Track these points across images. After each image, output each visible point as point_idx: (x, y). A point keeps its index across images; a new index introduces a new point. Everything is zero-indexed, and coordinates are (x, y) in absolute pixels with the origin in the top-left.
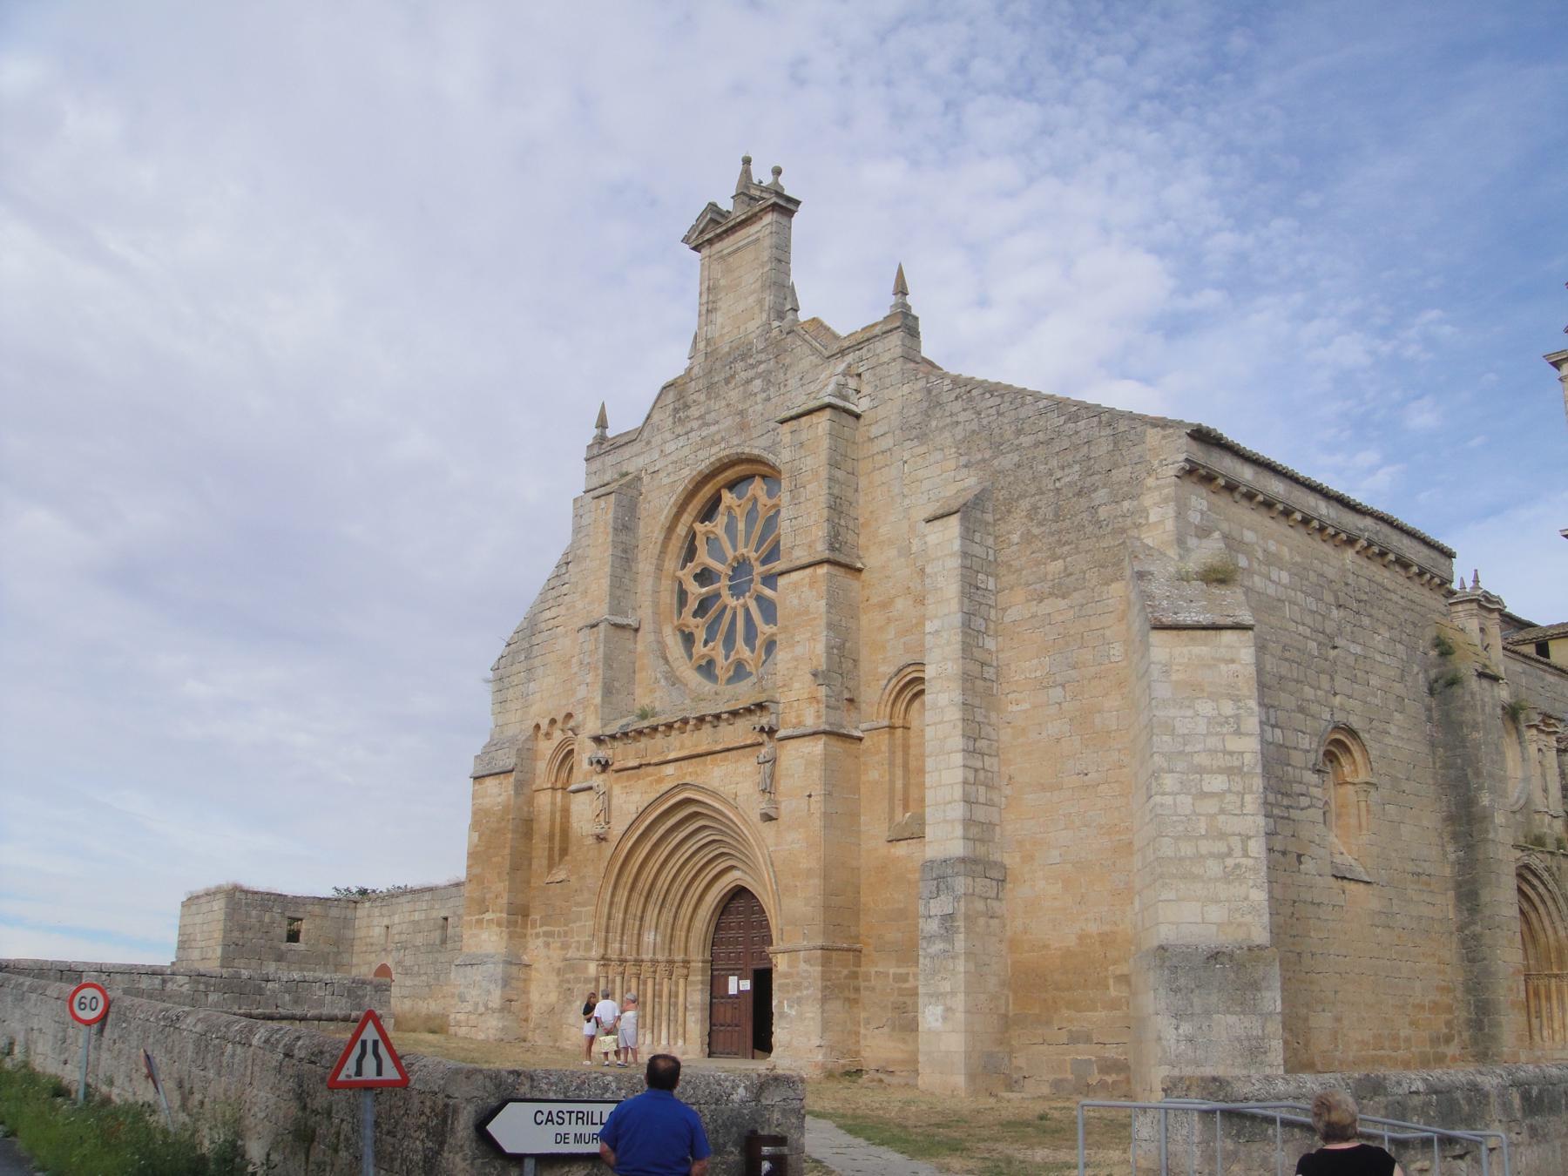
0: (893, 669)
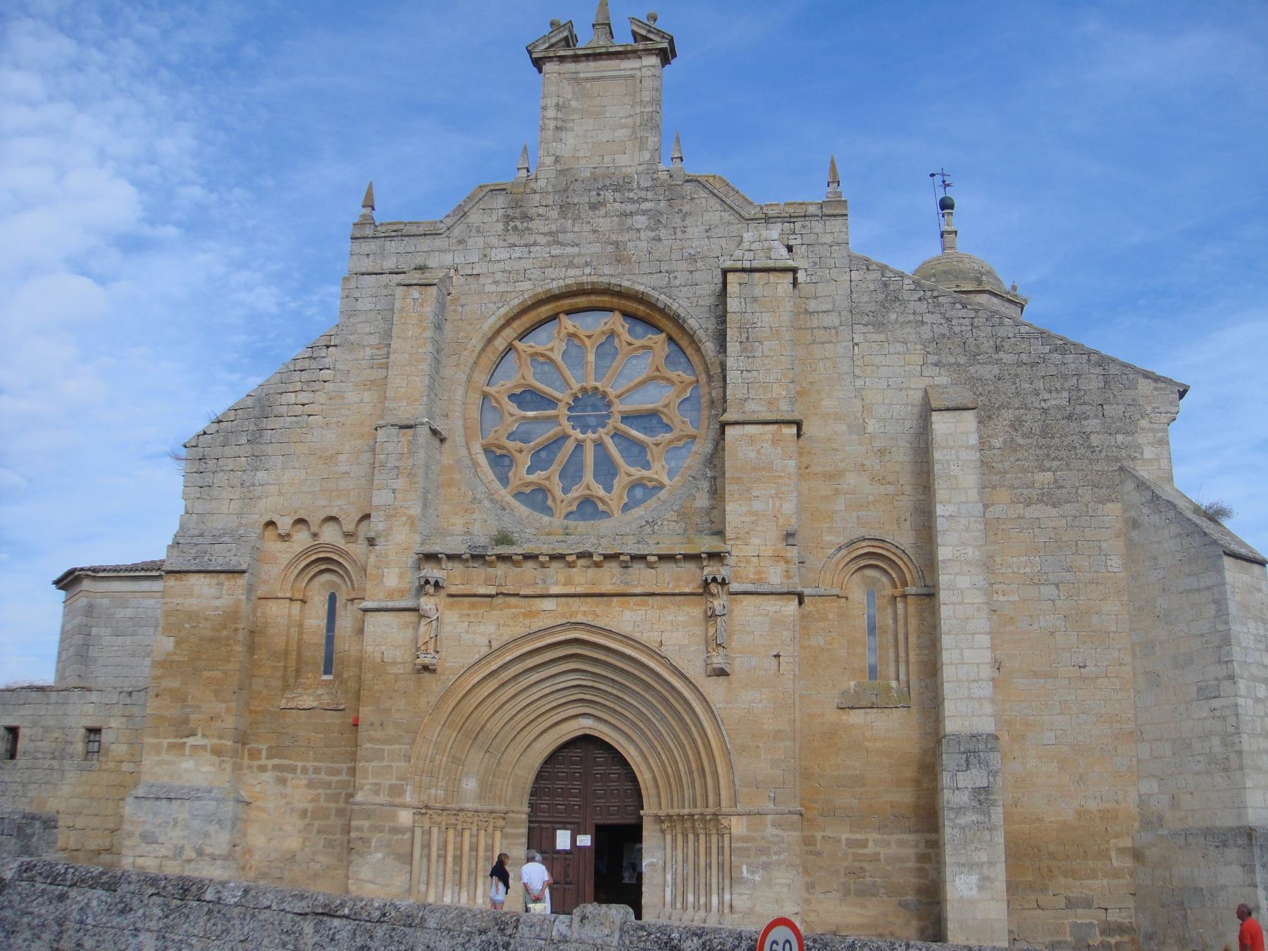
0: (842, 540)
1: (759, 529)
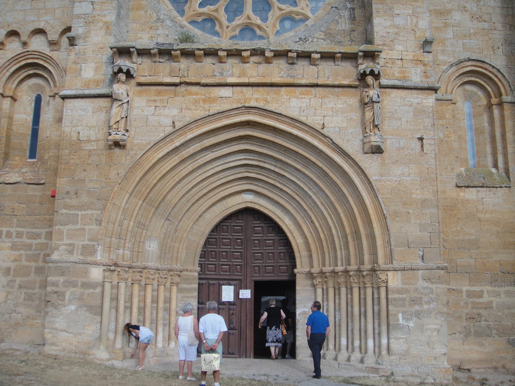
0: (452, 60)
1: (401, 38)
